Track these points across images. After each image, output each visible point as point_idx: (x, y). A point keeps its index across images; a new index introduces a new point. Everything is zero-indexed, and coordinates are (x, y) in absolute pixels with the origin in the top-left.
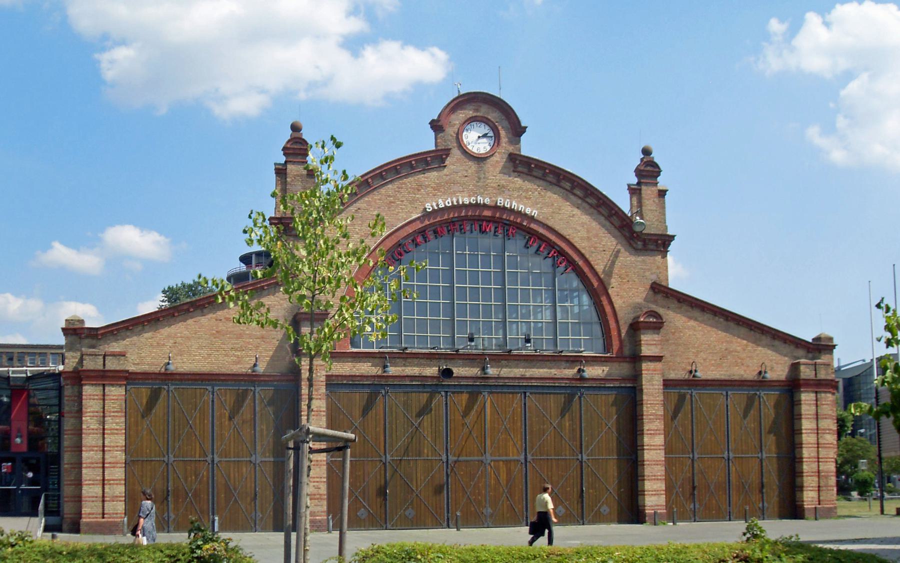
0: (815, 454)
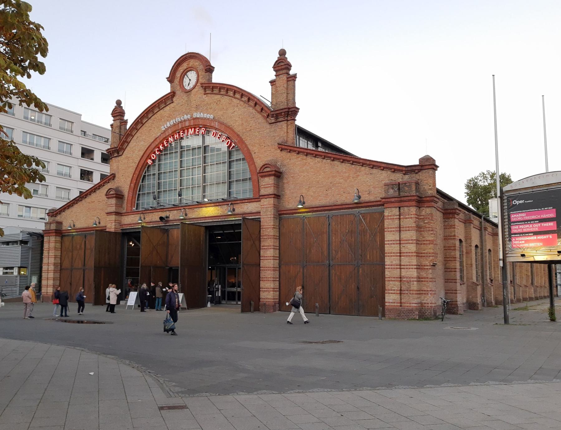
0: (398, 262)
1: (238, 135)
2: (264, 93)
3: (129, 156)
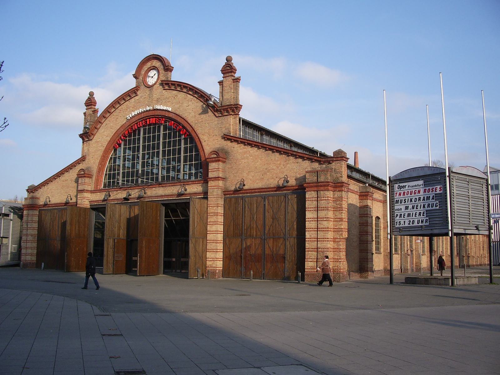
2: (213, 90)
3: (98, 140)
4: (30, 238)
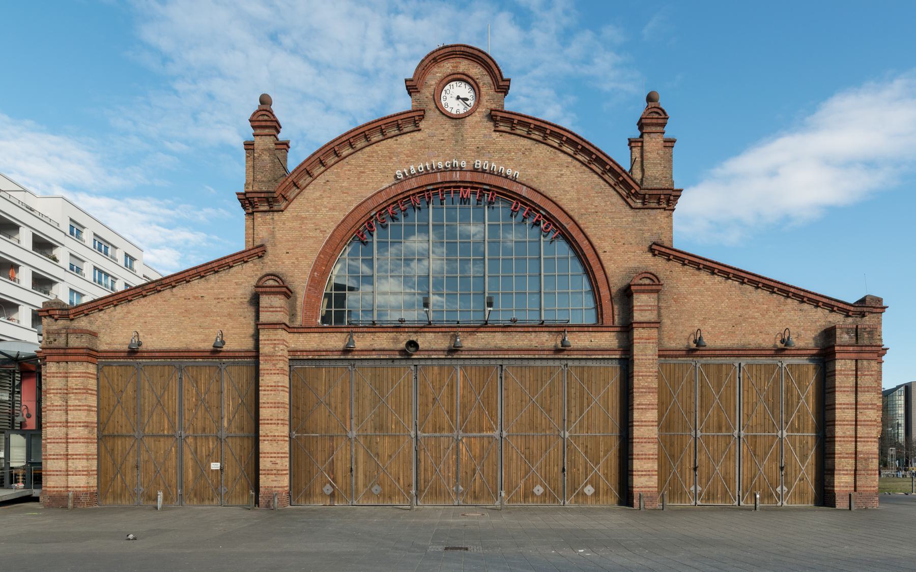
1: (571, 217)
4: (78, 432)
